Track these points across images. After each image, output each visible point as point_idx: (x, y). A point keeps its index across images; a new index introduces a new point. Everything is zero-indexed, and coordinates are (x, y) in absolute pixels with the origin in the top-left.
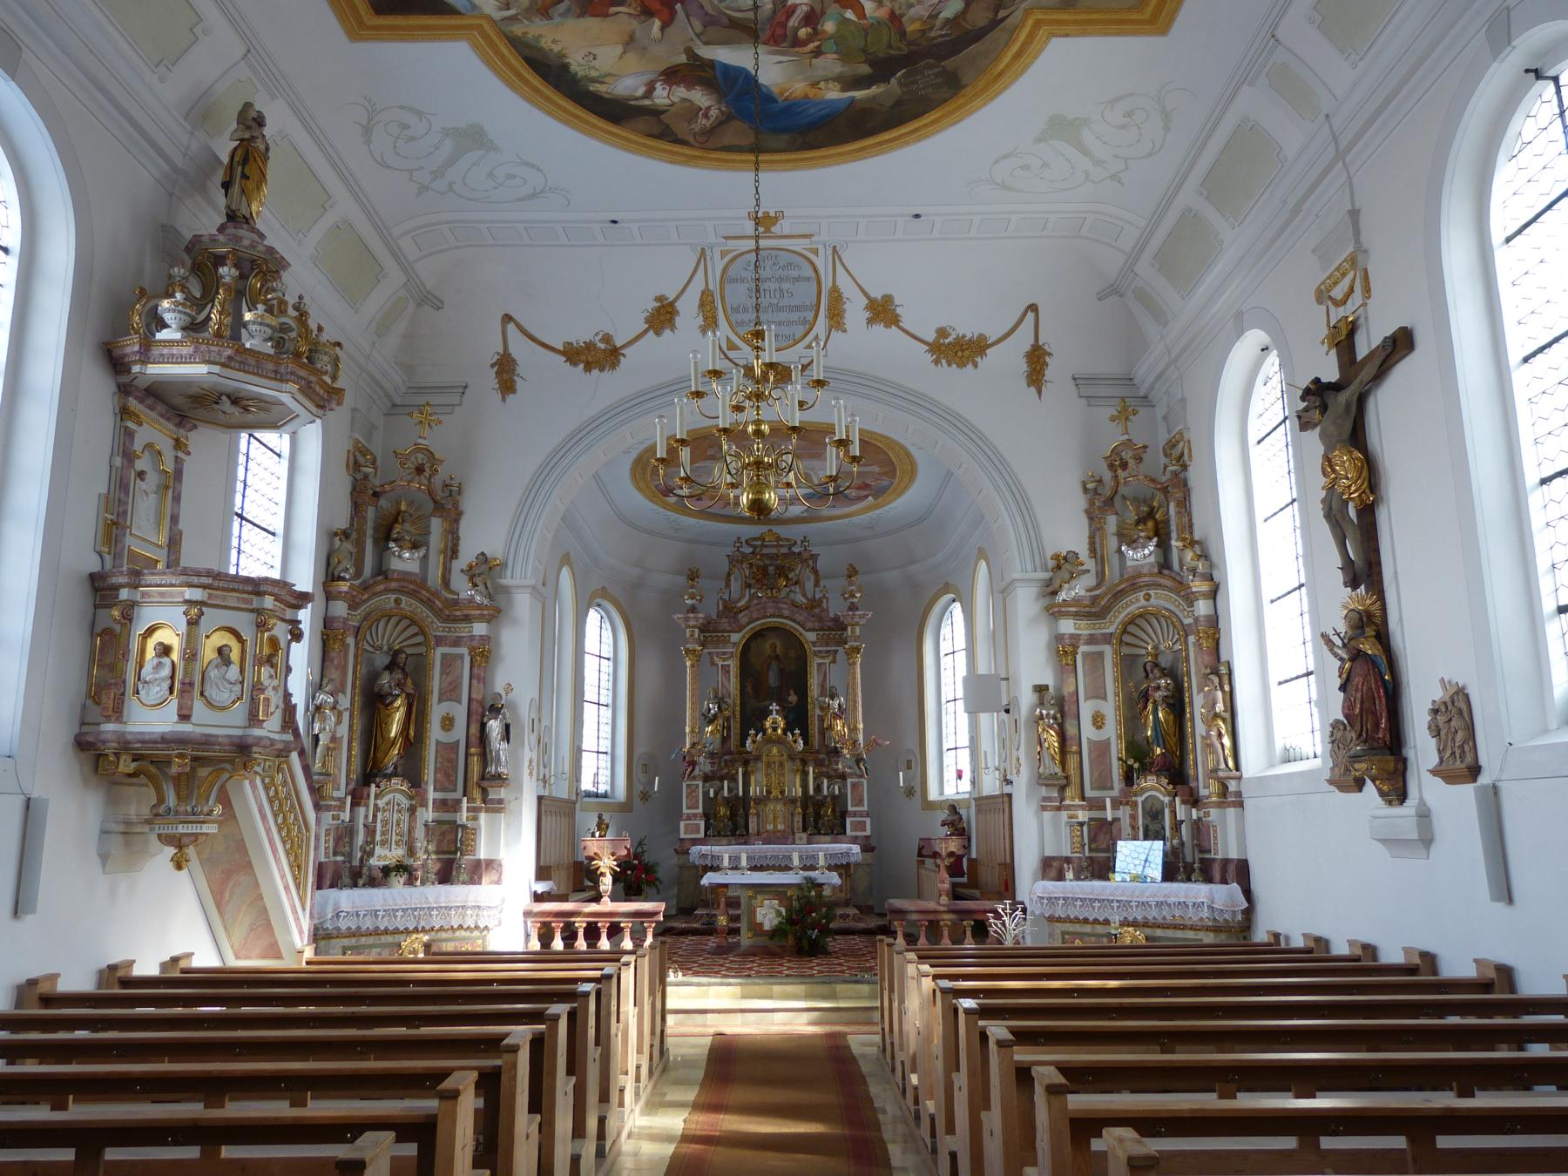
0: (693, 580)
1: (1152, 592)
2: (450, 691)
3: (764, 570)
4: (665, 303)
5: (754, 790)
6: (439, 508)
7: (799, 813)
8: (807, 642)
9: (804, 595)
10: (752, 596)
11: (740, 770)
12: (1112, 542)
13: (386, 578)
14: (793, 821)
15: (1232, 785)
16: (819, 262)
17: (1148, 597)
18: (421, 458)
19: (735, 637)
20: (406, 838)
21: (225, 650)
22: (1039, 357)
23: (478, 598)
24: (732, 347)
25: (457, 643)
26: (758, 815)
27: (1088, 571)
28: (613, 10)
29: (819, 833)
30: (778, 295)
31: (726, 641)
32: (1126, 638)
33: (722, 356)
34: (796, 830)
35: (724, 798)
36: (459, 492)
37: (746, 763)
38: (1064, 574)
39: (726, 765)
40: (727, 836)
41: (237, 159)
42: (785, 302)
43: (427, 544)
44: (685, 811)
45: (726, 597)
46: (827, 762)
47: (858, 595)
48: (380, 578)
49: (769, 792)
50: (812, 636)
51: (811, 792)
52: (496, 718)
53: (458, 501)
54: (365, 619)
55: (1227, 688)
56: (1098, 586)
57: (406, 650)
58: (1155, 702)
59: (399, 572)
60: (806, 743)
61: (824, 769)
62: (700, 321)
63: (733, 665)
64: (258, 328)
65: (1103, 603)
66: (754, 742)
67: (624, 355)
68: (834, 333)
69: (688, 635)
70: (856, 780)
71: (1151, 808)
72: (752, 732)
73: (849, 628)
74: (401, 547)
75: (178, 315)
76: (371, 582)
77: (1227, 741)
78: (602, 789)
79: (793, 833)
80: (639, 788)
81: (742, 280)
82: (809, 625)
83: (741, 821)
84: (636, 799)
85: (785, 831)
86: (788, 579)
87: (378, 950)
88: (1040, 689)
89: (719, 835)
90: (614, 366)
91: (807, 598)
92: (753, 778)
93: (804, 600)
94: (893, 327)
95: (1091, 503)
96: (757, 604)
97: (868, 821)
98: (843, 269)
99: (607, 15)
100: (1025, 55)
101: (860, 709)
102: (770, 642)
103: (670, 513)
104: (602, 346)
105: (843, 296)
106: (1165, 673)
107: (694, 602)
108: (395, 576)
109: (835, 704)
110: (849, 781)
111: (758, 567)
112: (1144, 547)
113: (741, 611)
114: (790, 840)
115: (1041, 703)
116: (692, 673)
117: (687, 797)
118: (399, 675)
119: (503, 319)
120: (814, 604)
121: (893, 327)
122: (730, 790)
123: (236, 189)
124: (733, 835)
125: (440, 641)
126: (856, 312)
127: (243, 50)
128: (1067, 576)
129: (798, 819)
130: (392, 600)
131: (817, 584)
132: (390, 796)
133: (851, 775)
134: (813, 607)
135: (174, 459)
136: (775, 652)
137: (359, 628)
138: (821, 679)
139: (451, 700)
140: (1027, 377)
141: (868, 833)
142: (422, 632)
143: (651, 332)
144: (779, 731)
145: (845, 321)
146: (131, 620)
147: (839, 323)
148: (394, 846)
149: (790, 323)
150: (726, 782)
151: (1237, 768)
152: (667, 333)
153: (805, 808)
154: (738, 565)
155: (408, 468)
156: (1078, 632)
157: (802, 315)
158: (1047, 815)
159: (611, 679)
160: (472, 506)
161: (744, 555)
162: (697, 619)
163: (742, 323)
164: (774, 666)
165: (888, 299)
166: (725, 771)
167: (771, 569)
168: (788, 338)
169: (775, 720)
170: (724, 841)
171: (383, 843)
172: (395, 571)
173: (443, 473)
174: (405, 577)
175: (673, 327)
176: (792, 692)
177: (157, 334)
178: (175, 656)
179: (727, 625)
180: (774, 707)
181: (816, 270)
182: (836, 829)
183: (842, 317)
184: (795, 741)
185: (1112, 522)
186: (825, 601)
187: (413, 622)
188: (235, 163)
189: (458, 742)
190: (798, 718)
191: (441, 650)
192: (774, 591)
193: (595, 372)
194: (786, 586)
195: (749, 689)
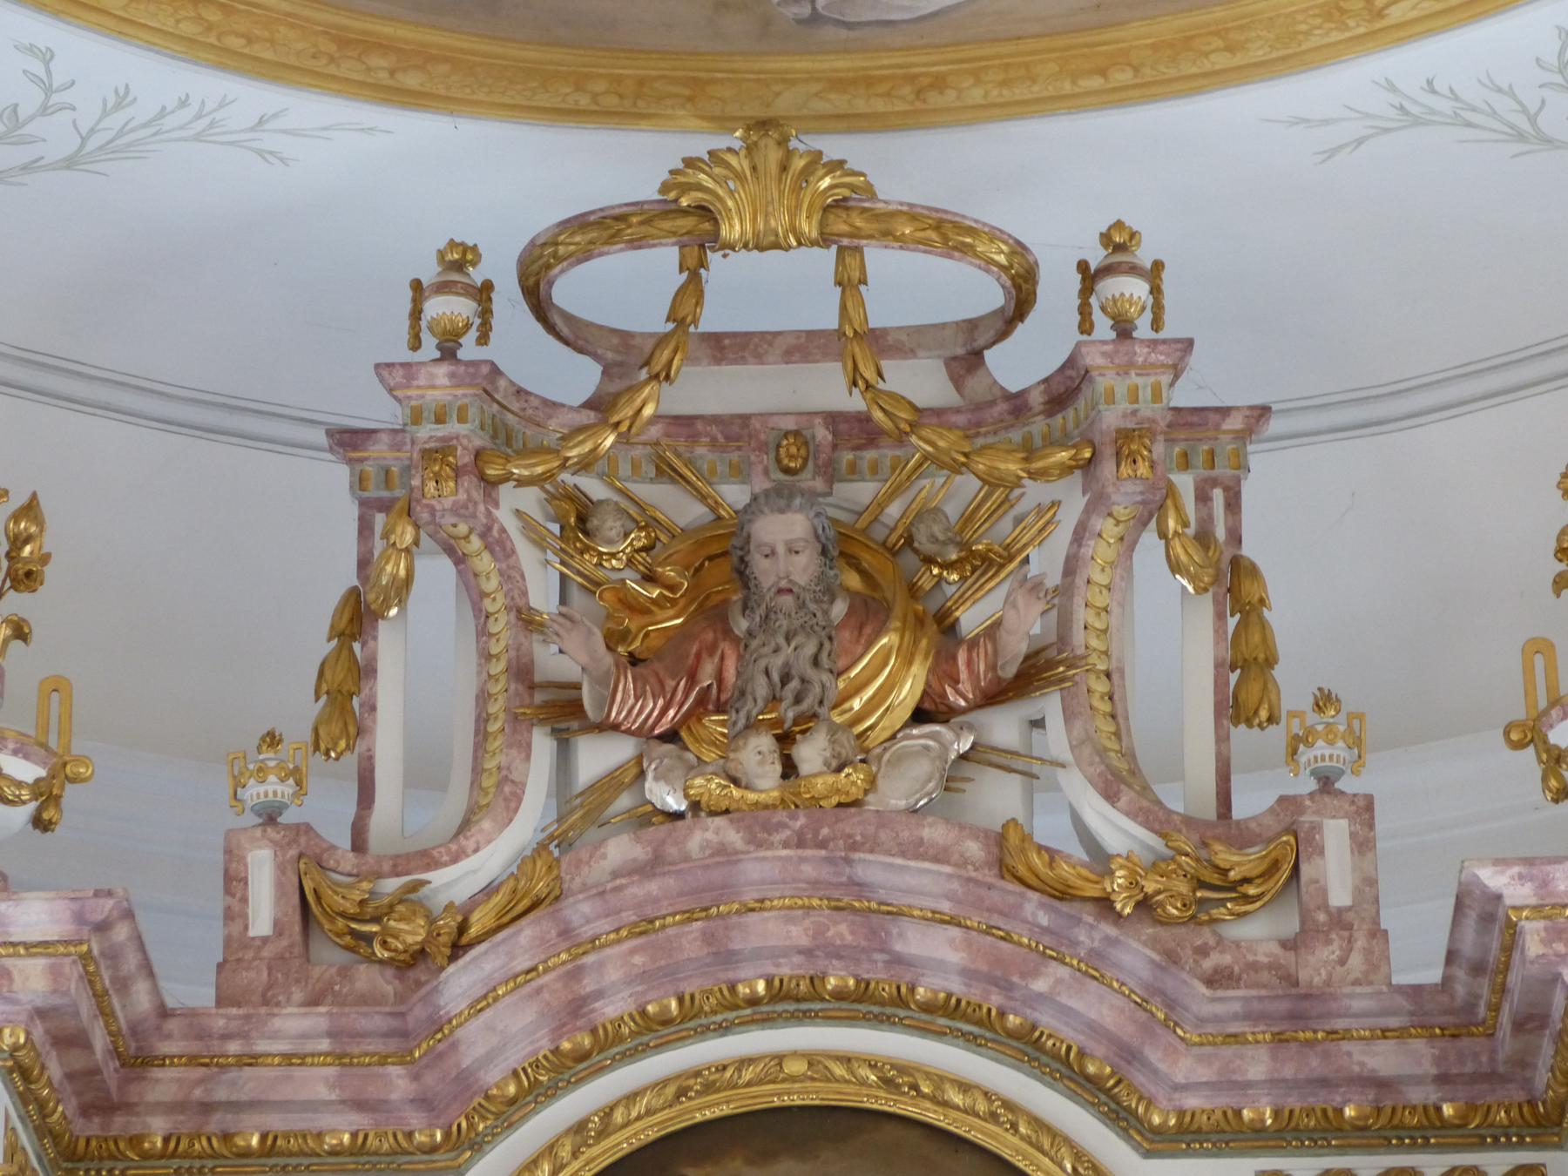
91: (1153, 816)
154: (445, 496)
179: (318, 1083)
186: (1336, 833)
192: (811, 753)
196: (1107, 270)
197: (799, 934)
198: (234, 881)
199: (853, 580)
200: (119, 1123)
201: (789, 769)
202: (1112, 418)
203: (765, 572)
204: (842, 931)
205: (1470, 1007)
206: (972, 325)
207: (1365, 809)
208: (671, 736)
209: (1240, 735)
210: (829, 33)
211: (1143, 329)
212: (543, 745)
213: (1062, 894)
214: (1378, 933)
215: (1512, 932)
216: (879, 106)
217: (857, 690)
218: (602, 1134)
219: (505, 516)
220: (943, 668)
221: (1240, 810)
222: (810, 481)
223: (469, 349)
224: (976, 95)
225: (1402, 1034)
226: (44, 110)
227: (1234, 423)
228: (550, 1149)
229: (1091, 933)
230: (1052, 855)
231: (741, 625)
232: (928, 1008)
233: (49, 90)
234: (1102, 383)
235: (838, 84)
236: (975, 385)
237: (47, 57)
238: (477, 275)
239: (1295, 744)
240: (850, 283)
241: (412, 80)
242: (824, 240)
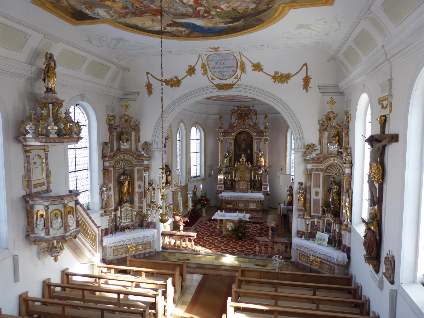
0: (221, 119)
1: (336, 159)
2: (140, 178)
3: (242, 116)
4: (192, 67)
6: (133, 129)
7: (249, 184)
8: (253, 136)
9: (253, 122)
12: (326, 141)
13: (120, 151)
14: (247, 186)
15: (349, 226)
16: (236, 55)
17: (334, 160)
18: (126, 117)
19: (233, 134)
20: (130, 217)
21: (57, 215)
22: (307, 80)
23: (145, 155)
24: (212, 79)
25: (140, 166)
26: (238, 184)
27: (317, 150)
28: (144, 15)
29: (254, 190)
30: (225, 64)
31: (231, 135)
32: (327, 171)
33: (210, 82)
35: (229, 179)
36: (139, 124)
37: (235, 170)
38: (310, 150)
39: (230, 169)
41: (46, 71)
42: (227, 65)
43: (131, 140)
46: (258, 170)
47: (267, 124)
48: (118, 151)
50: (255, 134)
52: (151, 187)
53: (139, 127)
54: (115, 163)
55: (350, 198)
56: (320, 153)
57: (127, 170)
58: (333, 192)
59: (123, 149)
62: (202, 72)
63: (233, 142)
64: (52, 131)
65: (321, 160)
66: (237, 165)
67: (181, 82)
68: (243, 74)
69: (219, 135)
71: (328, 223)
72: (237, 162)
73: (265, 133)
74: (123, 142)
75: (31, 130)
76: (116, 153)
77: (348, 214)
78: (198, 175)
79: (247, 189)
80: (208, 174)
81: (213, 61)
82: (254, 131)
85: (245, 189)
86: (248, 117)
87: (122, 249)
88: (300, 184)
90: (179, 85)
94: (261, 71)
95: (320, 128)
96: (239, 125)
98: (243, 56)
99: (143, 16)
100: (282, 14)
101: (267, 156)
102: (243, 135)
104: (175, 80)
105: (245, 63)
106: (336, 184)
107: (221, 125)
108: (122, 150)
111: (240, 114)
112: (334, 146)
113: (234, 127)
114: (246, 192)
115: (300, 189)
118: (125, 176)
119: (147, 73)
120: (255, 124)
121: (261, 71)
123: (46, 80)
124: (231, 189)
125: (136, 166)
126: (249, 68)
127: (43, 36)
128: (310, 152)
129: (249, 186)
130: (123, 156)
132: (125, 208)
133: (264, 175)
134: (255, 126)
135: (44, 154)
136: (244, 138)
137: (114, 165)
138: (257, 146)
139: (140, 181)
140: (303, 86)
142: (131, 163)
143: (189, 75)
144: (244, 162)
145: (246, 70)
146: (33, 209)
147: (244, 71)
148: (127, 219)
149: (229, 71)
151: (351, 221)
152: (193, 75)
153: (251, 183)
155: (123, 121)
156: (313, 168)
157: (233, 69)
158: (300, 219)
159: (200, 145)
160: (143, 127)
162: (221, 130)
163: (215, 72)
164: (244, 142)
165: (259, 64)
166: (230, 171)
167: (243, 115)
168: (229, 76)
169: (243, 159)
170: (229, 191)
171: (124, 219)
172: (122, 149)
173: (133, 120)
174: (125, 151)
175: (195, 74)
176: (249, 150)
177: (27, 136)
178: (44, 217)
181: (235, 57)
182: (259, 189)
183: (245, 69)
184: (249, 165)
185: (326, 134)
186: (258, 124)
187: (129, 161)
188: (46, 73)
189: (142, 192)
190: (250, 158)
191: (136, 168)
192: (244, 121)
193: (174, 87)
194: (247, 119)
195: (237, 149)
198: (228, 125)
207: (259, 123)
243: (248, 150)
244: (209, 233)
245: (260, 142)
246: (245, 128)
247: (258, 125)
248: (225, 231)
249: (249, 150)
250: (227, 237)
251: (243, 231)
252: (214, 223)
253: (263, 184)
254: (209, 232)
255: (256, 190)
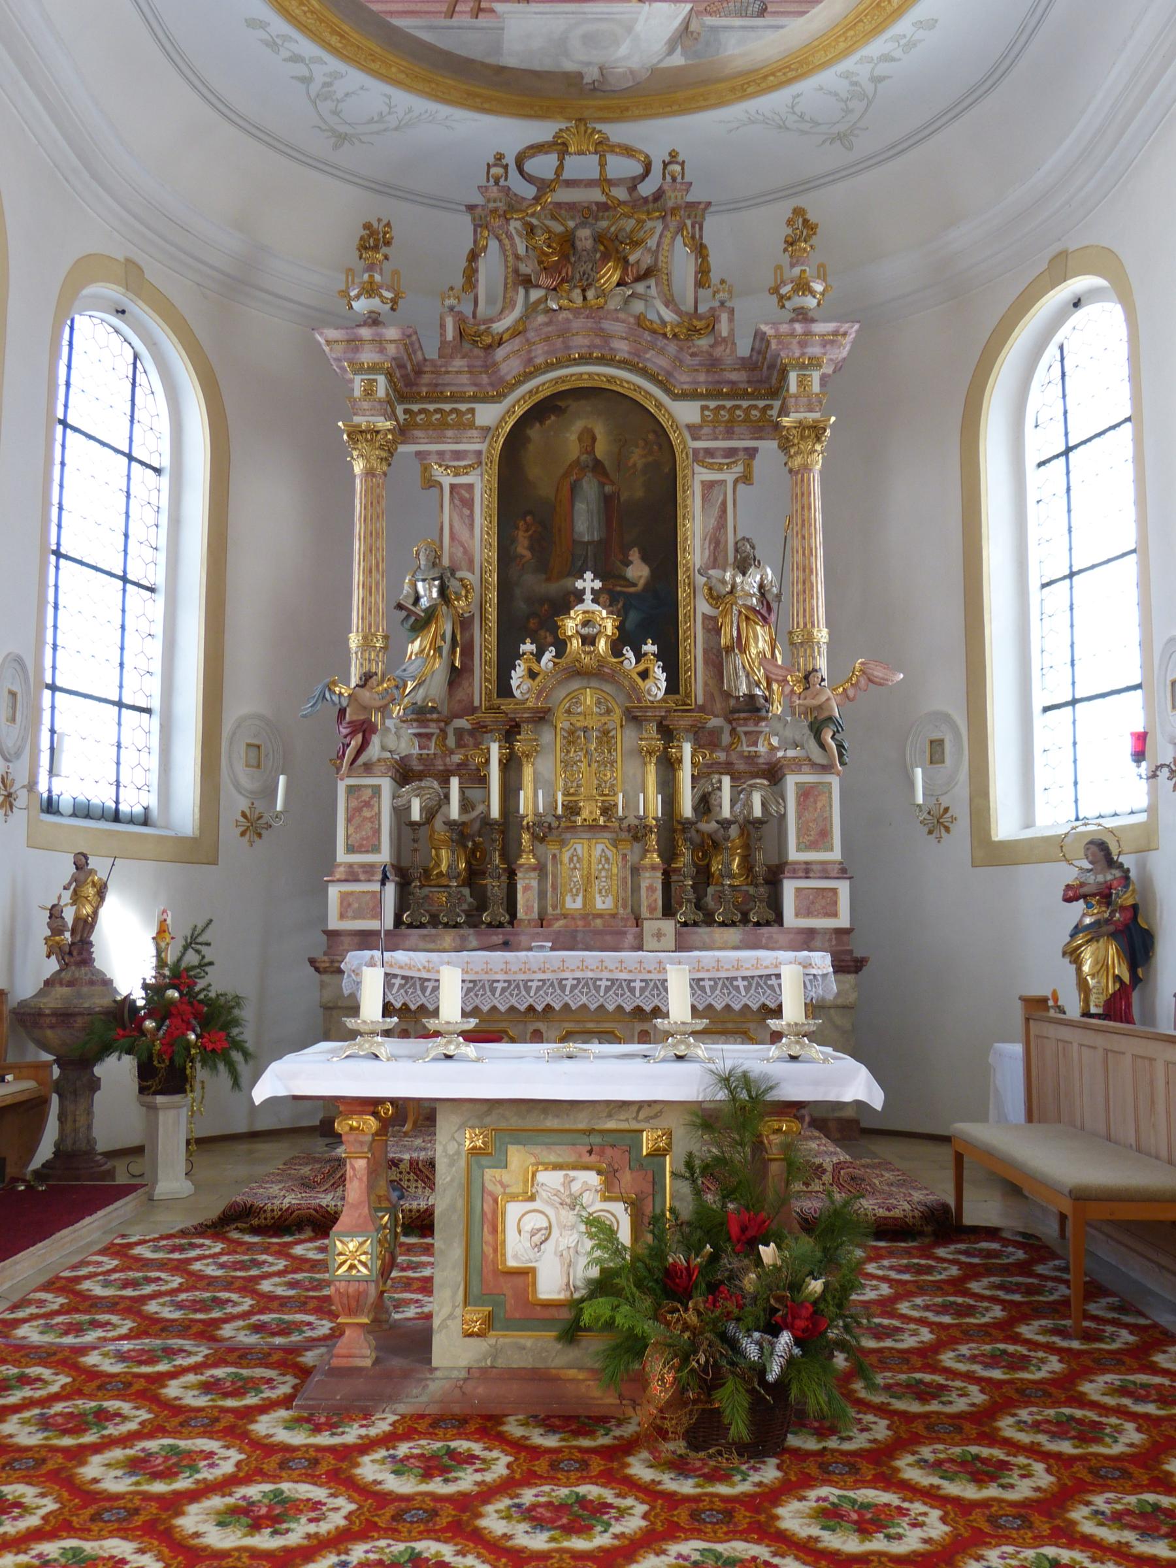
3: (568, 242)
5: (529, 802)
7: (654, 868)
9: (669, 302)
10: (531, 309)
11: (495, 748)
14: (636, 889)
19: (487, 414)
26: (541, 869)
29: (709, 921)
31: (465, 424)
34: (645, 912)
35: (450, 824)
37: (510, 733)
39: (460, 744)
40: (456, 926)
44: (342, 856)
45: (467, 309)
46: (726, 739)
49: (572, 810)
50: (687, 412)
51: (687, 809)
60: (673, 687)
61: (721, 756)
66: (532, 675)
69: (357, 393)
70: (809, 778)
73: (793, 377)
78: (131, 804)
79: (638, 922)
80: (235, 804)
82: (683, 380)
83: (494, 886)
84: (229, 831)
85: (614, 916)
89: (435, 922)
91: (678, 312)
92: (528, 772)
93: (668, 315)
97: (843, 888)
101: (820, 589)
102: (579, 425)
103: (307, 47)
109: (752, 581)
110: (791, 782)
114: (630, 939)
116: (368, 491)
117: (349, 820)
122: (466, 806)
124: (473, 922)
129: (652, 881)
131: (703, 277)
133: (797, 765)
134: (694, 331)
136: (591, 451)
138: (712, 522)
141: (843, 920)
144: (602, 645)
150: (455, 782)
153: (669, 854)
154: (496, 223)
159: (164, 520)
161: (513, 205)
162: (379, 343)
164: (590, 488)
166: (457, 758)
167: (584, 234)
170: (449, 938)
176: (634, 555)
179: (464, 379)
180: (589, 583)
184: (644, 675)
186: (724, 317)
192: (590, 294)
195: (522, 548)
196: (670, 163)
197: (586, 342)
198: (443, 326)
199: (602, 248)
200: (414, 389)
201: (585, 298)
202: (670, 204)
203: (578, 244)
204: (598, 341)
205: (757, 362)
206: (634, 178)
207: (732, 311)
208: (554, 289)
209: (701, 291)
210: (599, 94)
211: (679, 179)
212: (521, 291)
213: (654, 332)
214: (734, 344)
215: (768, 342)
216: (611, 115)
217: (603, 276)
218: (537, 393)
219: (511, 228)
220: (625, 272)
221: (699, 311)
222: (591, 220)
223: (502, 182)
224: (637, 112)
225: (738, 370)
226: (389, 113)
227: (702, 206)
228: (523, 397)
229: (661, 342)
230: (651, 322)
231: (573, 259)
232: (619, 362)
233: (390, 107)
234: (668, 194)
235: (600, 109)
236: (635, 194)
237: (390, 97)
238: (504, 162)
239: (715, 293)
240: (602, 165)
241: (486, 106)
242: (596, 153)
243: (628, 563)
244: (196, 1369)
245: (740, 486)
246: (603, 360)
247: (724, 328)
248: (476, 1316)
249: (634, 555)
250: (514, 1429)
251: (816, 1286)
252: (282, 1252)
253: (794, 855)
254: (201, 1352)
255: (723, 924)
